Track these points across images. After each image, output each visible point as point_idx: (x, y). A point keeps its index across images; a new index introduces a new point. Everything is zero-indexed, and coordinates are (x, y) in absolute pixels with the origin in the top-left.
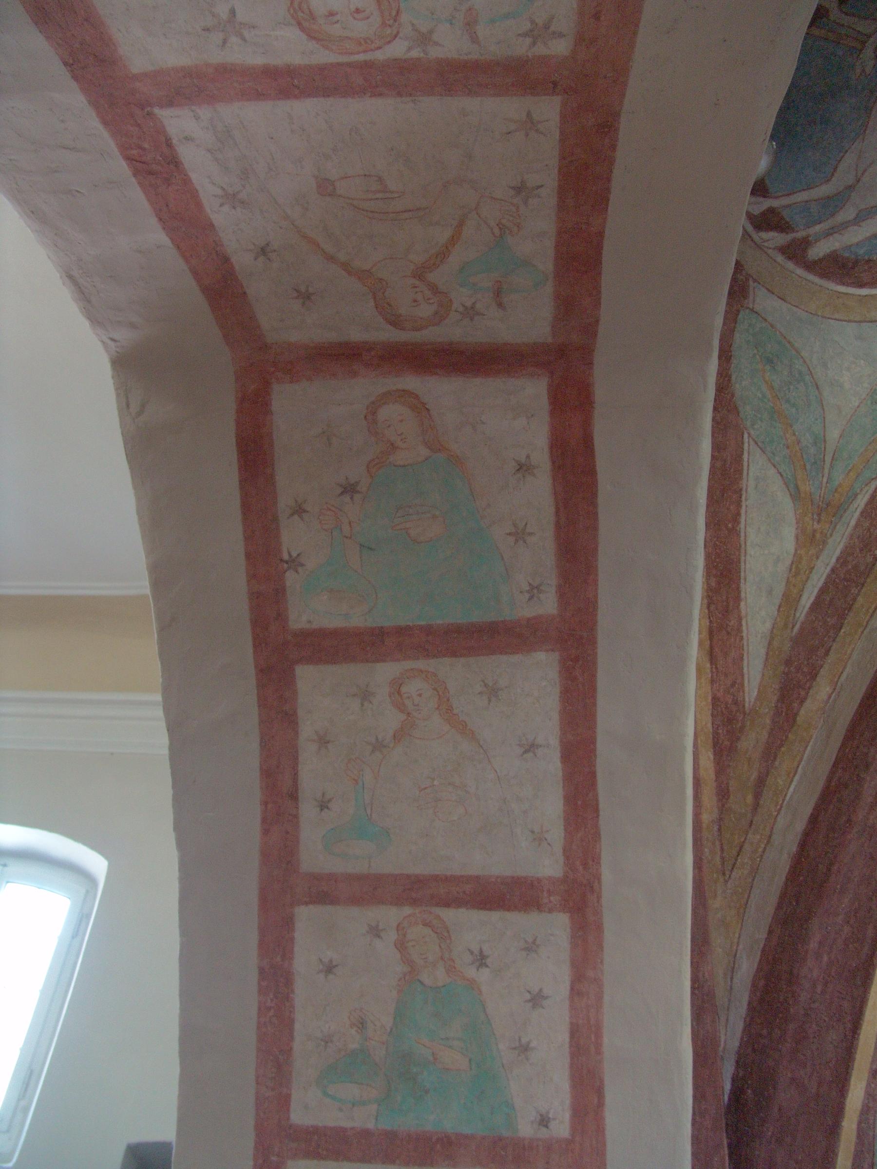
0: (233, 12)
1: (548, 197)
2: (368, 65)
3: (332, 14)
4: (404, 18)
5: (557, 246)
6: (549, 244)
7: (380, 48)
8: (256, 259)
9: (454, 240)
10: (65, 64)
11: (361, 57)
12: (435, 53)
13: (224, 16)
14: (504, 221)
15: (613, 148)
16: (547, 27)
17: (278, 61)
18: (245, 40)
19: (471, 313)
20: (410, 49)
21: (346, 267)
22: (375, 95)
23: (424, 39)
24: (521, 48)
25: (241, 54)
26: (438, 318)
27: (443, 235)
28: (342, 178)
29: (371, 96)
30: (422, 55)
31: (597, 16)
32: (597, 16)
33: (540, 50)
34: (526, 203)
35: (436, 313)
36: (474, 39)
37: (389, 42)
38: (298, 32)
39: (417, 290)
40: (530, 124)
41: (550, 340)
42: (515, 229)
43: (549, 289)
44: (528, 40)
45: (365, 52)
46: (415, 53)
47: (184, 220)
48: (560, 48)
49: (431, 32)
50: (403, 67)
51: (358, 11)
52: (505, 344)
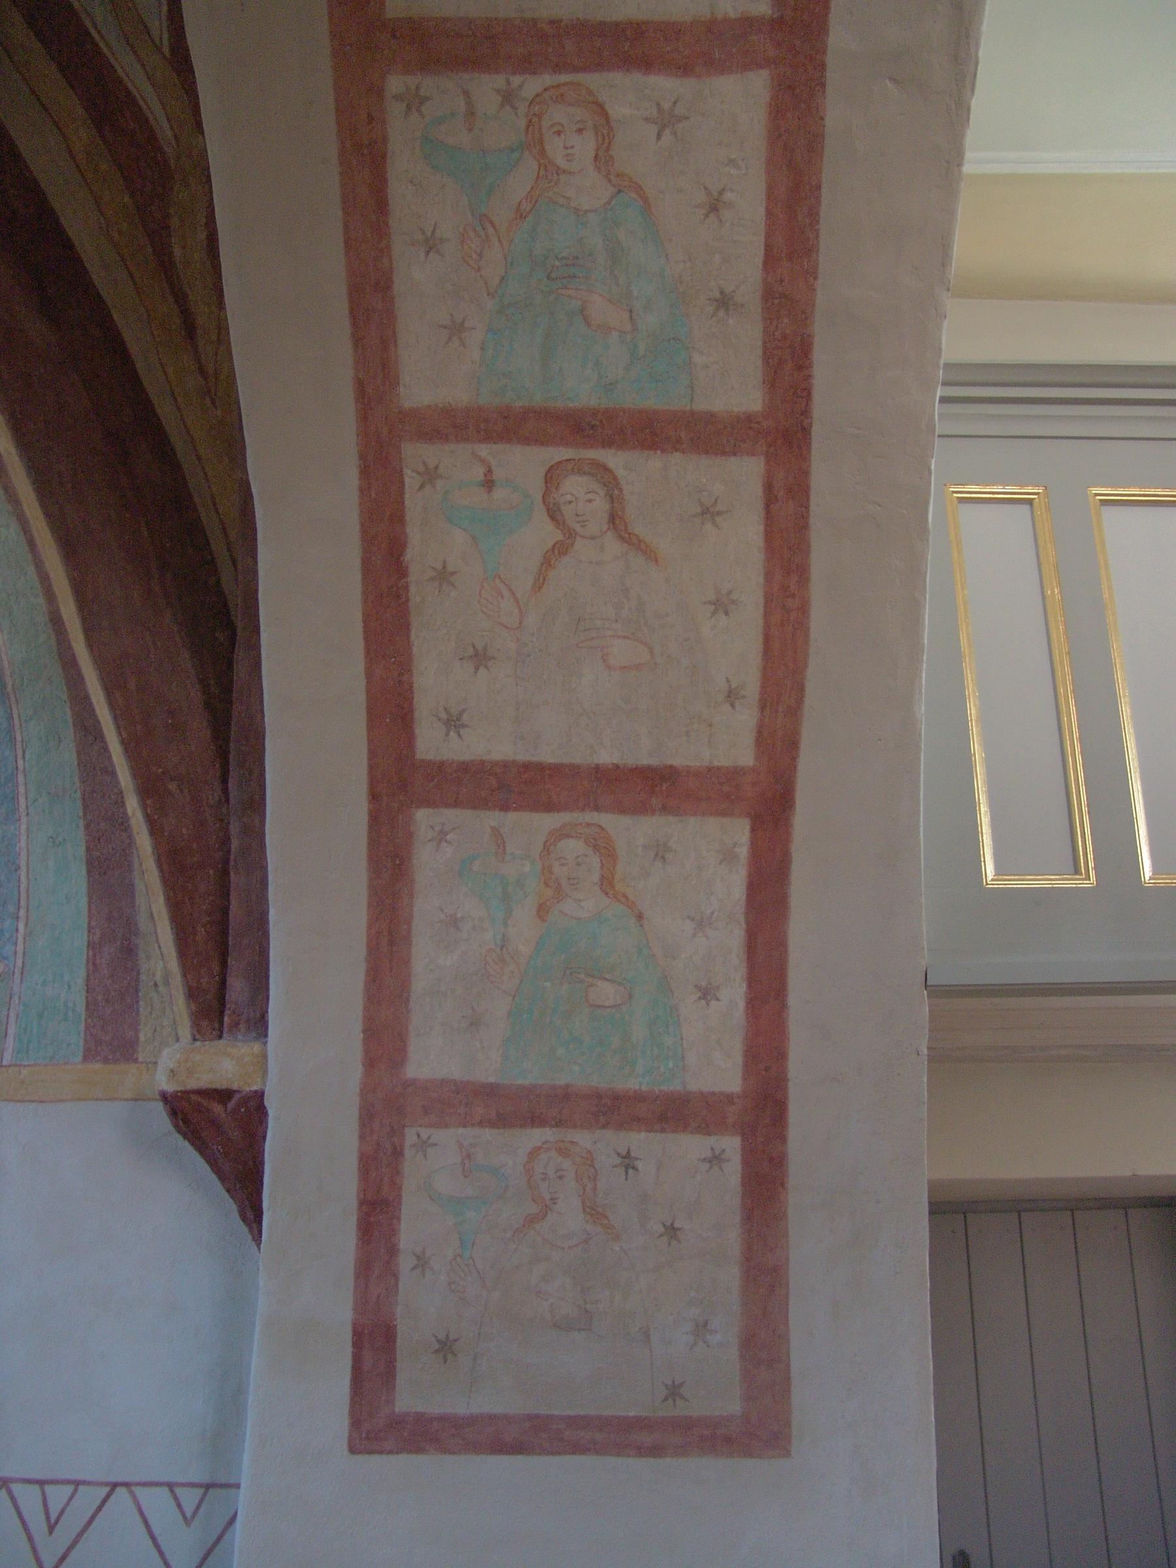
0: (659, 136)
2: (557, 68)
3: (580, 131)
4: (523, 123)
10: (823, 85)
11: (564, 78)
12: (499, 80)
13: (667, 131)
16: (409, 107)
18: (658, 104)
20: (521, 86)
23: (508, 97)
24: (428, 84)
25: (663, 85)
29: (562, 20)
30: (512, 78)
33: (411, 81)
36: (466, 94)
37: (537, 95)
38: (610, 112)
44: (422, 92)
45: (558, 86)
46: (516, 80)
48: (395, 84)
49: (502, 106)
50: (527, 65)
51: (559, 133)
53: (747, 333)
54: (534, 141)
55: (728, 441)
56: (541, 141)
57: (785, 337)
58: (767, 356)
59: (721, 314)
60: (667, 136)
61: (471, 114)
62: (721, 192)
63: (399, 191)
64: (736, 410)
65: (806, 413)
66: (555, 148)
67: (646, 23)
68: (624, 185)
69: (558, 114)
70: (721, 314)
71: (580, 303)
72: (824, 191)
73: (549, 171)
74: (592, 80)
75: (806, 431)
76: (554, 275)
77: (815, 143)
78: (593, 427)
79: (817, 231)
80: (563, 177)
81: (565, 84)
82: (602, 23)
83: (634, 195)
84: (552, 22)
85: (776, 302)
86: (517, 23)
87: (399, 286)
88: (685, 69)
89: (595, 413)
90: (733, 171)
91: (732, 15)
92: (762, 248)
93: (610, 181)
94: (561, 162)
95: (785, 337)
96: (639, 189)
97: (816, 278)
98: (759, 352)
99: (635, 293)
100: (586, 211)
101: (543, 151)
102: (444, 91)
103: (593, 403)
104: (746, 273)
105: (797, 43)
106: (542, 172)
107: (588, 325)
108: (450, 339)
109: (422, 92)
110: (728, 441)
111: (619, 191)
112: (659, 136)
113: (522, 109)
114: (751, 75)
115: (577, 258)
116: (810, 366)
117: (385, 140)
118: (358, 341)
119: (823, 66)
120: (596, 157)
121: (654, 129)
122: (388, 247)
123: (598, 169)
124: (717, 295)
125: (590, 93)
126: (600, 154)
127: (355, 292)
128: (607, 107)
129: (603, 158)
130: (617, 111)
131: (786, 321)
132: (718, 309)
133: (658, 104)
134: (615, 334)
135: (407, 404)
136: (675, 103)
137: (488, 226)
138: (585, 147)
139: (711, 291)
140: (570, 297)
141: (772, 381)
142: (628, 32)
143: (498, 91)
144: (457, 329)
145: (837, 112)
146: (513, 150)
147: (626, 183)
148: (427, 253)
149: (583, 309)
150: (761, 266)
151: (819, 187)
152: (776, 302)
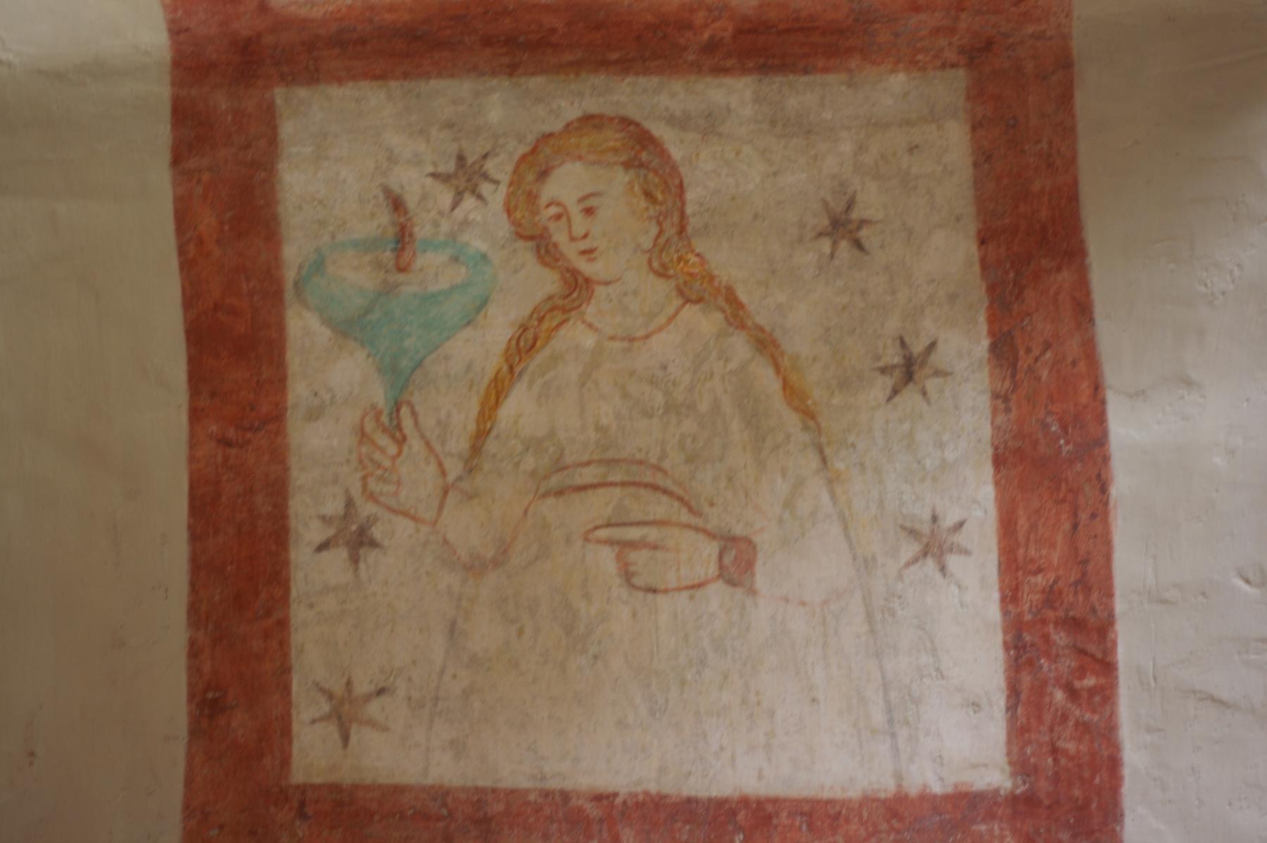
1: (310, 511)
5: (283, 380)
6: (298, 391)
8: (932, 346)
9: (497, 391)
14: (392, 449)
15: (194, 651)
19: (465, 177)
21: (735, 312)
22: (608, 797)
26: (537, 161)
27: (519, 407)
28: (700, 585)
29: (616, 795)
34: (349, 503)
35: (544, 175)
39: (583, 245)
40: (344, 713)
41: (279, 94)
42: (369, 426)
43: (294, 252)
47: (1053, 466)
52: (382, 77)
67: (775, 801)
82: (689, 800)
84: (598, 798)
86: (532, 798)
91: (937, 789)
142: (741, 816)
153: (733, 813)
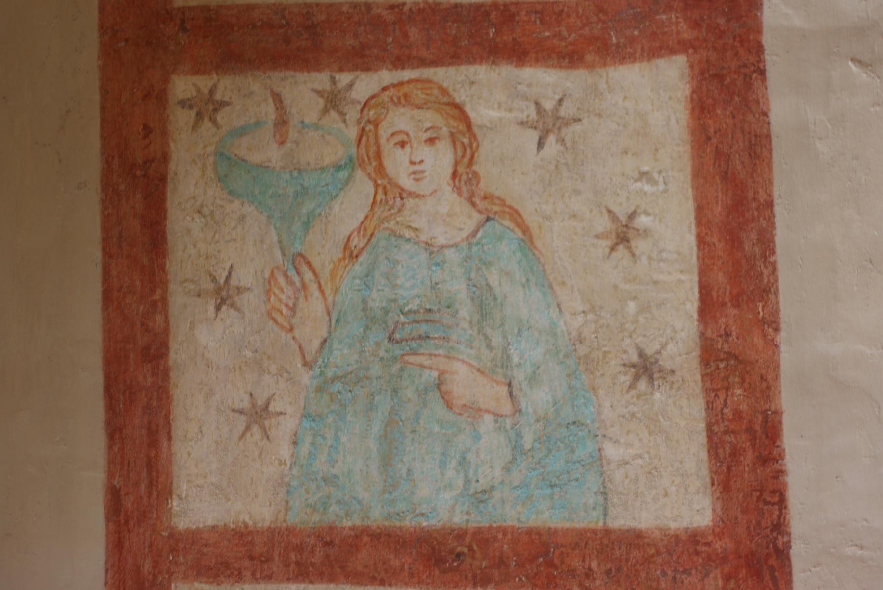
0: (540, 144)
2: (399, 63)
3: (431, 141)
4: (353, 133)
7: (384, 89)
10: (762, 72)
11: (407, 74)
12: (321, 79)
16: (199, 116)
17: (507, 71)
18: (537, 103)
20: (351, 86)
22: (398, 6)
23: (333, 101)
24: (226, 86)
29: (404, 4)
30: (337, 77)
31: (147, 130)
32: (147, 130)
33: (204, 83)
36: (277, 98)
37: (373, 97)
38: (472, 115)
44: (218, 97)
45: (401, 84)
46: (344, 78)
48: (182, 86)
49: (325, 111)
50: (361, 59)
51: (402, 144)
53: (682, 415)
54: (369, 156)
55: (664, 573)
56: (378, 155)
57: (738, 415)
58: (714, 444)
59: (642, 385)
60: (552, 146)
61: (282, 122)
62: (632, 216)
63: (183, 224)
64: (673, 525)
65: (780, 527)
66: (398, 164)
68: (493, 209)
69: (400, 120)
70: (642, 385)
71: (435, 374)
72: (777, 209)
73: (390, 194)
74: (442, 75)
75: (783, 554)
76: (397, 336)
77: (758, 146)
78: (458, 555)
79: (774, 265)
80: (410, 203)
81: (410, 81)
83: (507, 223)
84: (392, 7)
85: (722, 365)
86: (345, 9)
87: (177, 354)
88: (572, 58)
89: (460, 534)
90: (647, 188)
92: (696, 290)
93: (474, 205)
94: (407, 183)
95: (738, 415)
96: (516, 216)
97: (777, 330)
98: (703, 438)
99: (516, 359)
100: (442, 247)
101: (380, 169)
102: (248, 97)
103: (458, 520)
104: (675, 327)
105: (722, 21)
106: (380, 196)
107: (449, 406)
108: (248, 428)
109: (218, 97)
110: (664, 573)
111: (488, 219)
112: (540, 144)
113: (352, 114)
114: (661, 62)
115: (430, 310)
116: (781, 456)
117: (165, 158)
118: (114, 432)
119: (759, 49)
120: (455, 175)
121: (534, 136)
122: (164, 299)
123: (458, 190)
124: (635, 358)
125: (444, 91)
126: (461, 169)
127: (114, 362)
128: (468, 109)
129: (464, 176)
130: (482, 113)
131: (739, 392)
132: (637, 378)
133: (537, 103)
134: (488, 418)
135: (182, 524)
136: (561, 101)
137: (304, 268)
138: (439, 161)
139: (625, 352)
140: (422, 366)
141: (724, 481)
142: (493, 16)
143: (319, 93)
144: (259, 415)
145: (784, 106)
146: (338, 168)
147: (496, 208)
148: (218, 308)
149: (439, 385)
150: (695, 316)
151: (770, 204)
152: (722, 365)
153: (488, 14)
